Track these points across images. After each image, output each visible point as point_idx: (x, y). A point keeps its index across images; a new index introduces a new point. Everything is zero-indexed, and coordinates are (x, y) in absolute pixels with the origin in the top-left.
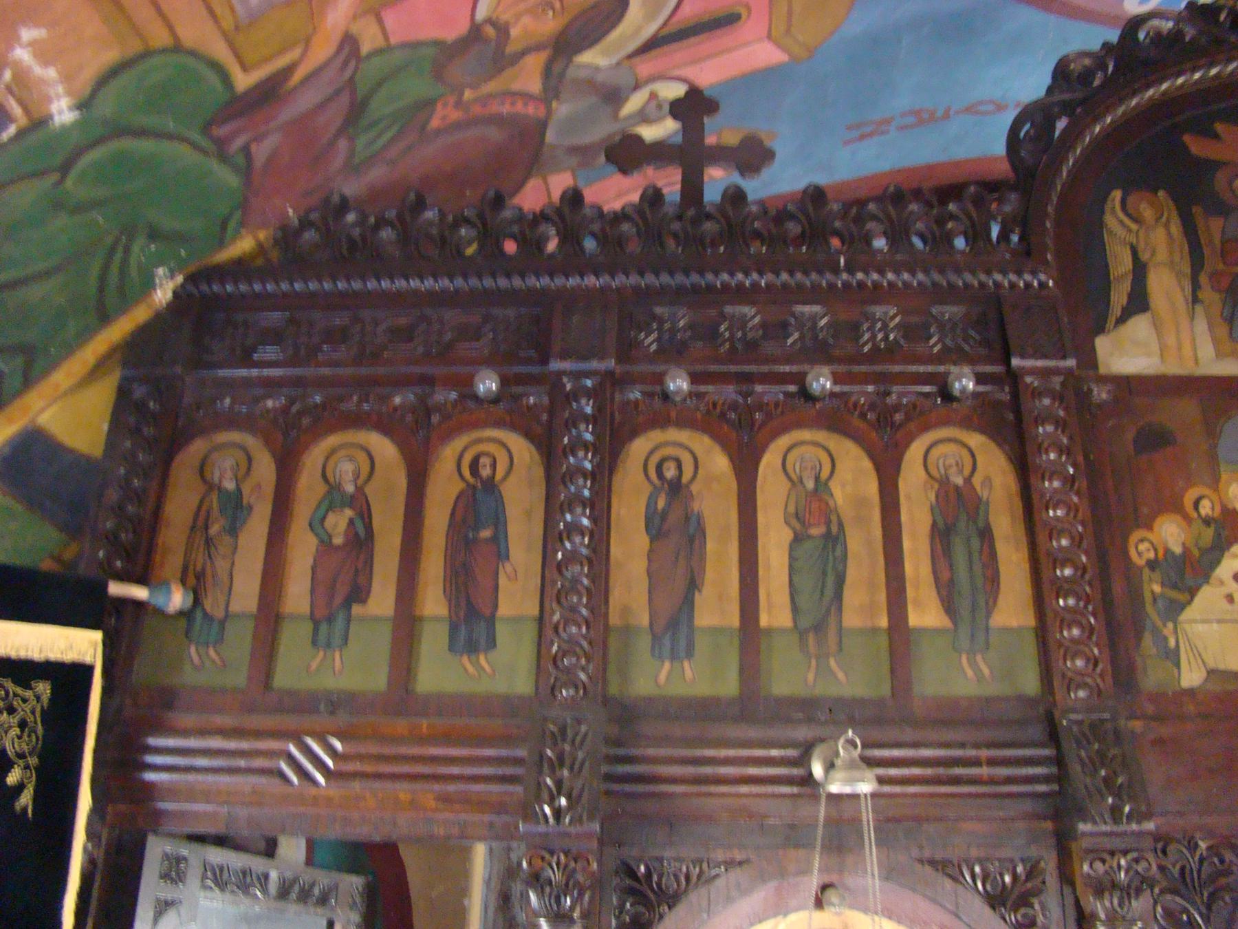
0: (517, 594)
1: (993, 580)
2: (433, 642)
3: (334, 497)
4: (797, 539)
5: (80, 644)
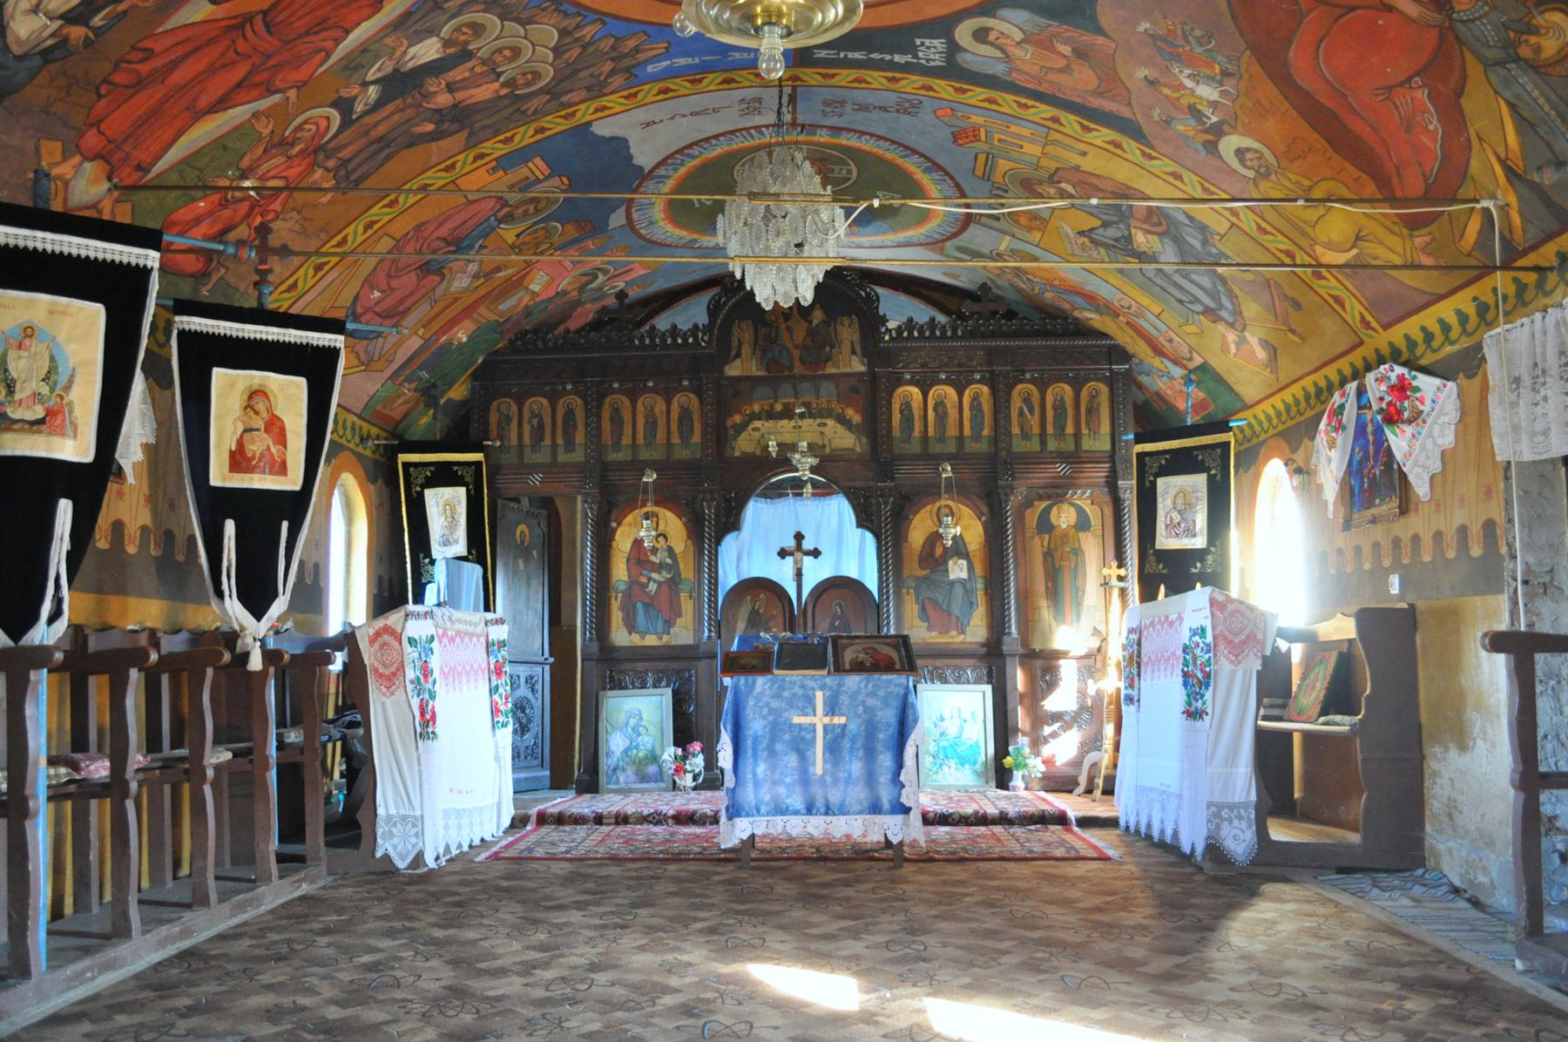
0: (580, 438)
2: (561, 450)
3: (533, 415)
5: (477, 457)
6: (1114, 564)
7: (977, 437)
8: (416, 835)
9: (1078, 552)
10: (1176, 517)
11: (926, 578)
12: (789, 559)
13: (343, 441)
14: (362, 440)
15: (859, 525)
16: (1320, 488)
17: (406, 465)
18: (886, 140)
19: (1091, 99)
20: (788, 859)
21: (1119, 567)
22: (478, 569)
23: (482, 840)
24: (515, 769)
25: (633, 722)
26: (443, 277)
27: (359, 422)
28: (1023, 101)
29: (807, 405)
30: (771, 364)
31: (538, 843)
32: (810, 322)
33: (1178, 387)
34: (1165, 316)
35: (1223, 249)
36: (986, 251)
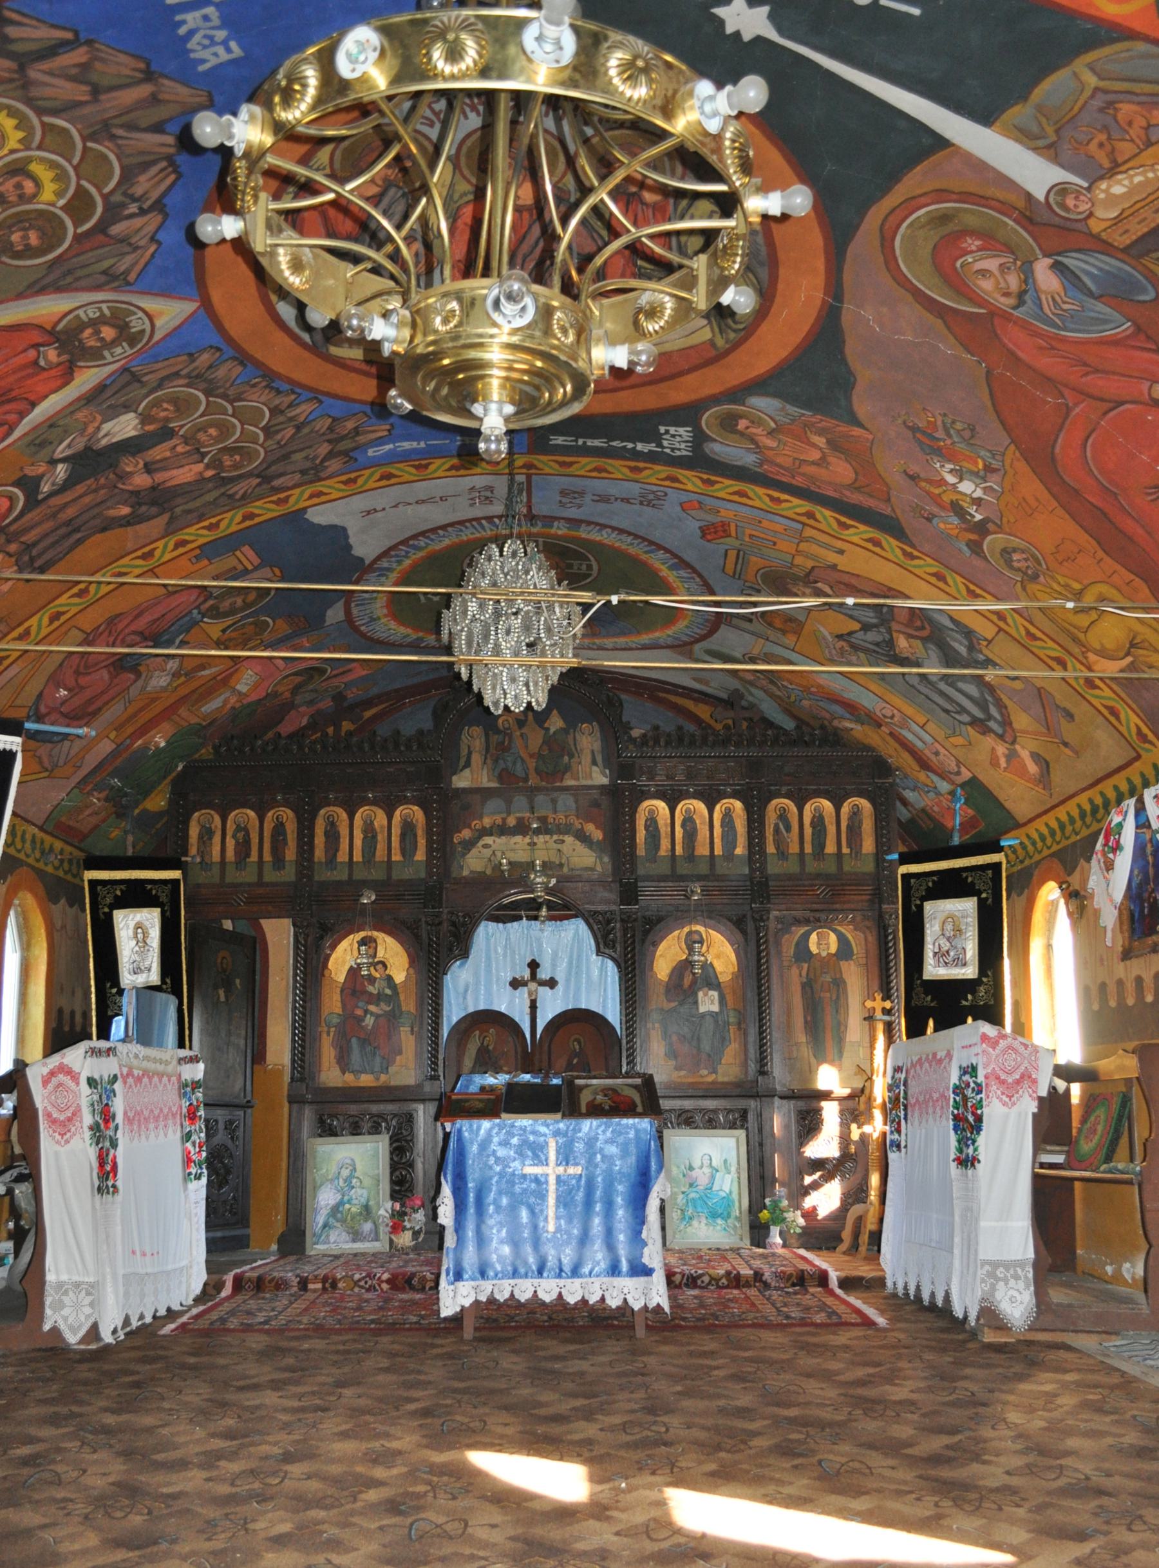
1: (416, 848)
3: (239, 828)
4: (365, 837)
5: (175, 874)
6: (878, 997)
7: (729, 855)
8: (91, 1305)
9: (839, 984)
10: (946, 946)
11: (674, 1010)
12: (524, 991)
13: (22, 856)
14: (43, 852)
15: (599, 952)
16: (1097, 913)
17: (93, 883)
18: (629, 534)
19: (848, 493)
20: (515, 1328)
21: (883, 999)
22: (172, 1002)
23: (169, 1310)
24: (209, 1226)
25: (345, 1173)
26: (138, 675)
27: (40, 835)
28: (776, 494)
29: (543, 820)
30: (504, 776)
31: (232, 1313)
32: (548, 729)
33: (945, 803)
34: (930, 727)
35: (991, 656)
36: (739, 655)
